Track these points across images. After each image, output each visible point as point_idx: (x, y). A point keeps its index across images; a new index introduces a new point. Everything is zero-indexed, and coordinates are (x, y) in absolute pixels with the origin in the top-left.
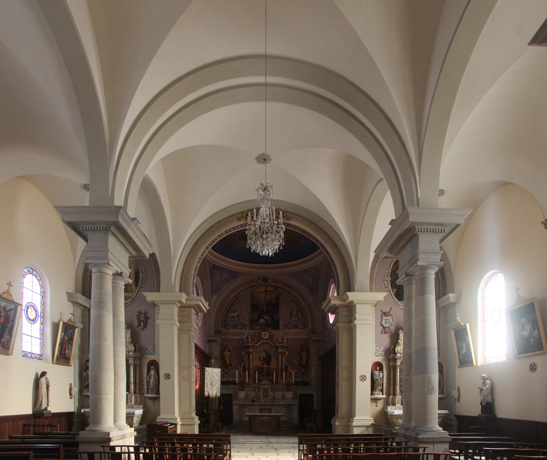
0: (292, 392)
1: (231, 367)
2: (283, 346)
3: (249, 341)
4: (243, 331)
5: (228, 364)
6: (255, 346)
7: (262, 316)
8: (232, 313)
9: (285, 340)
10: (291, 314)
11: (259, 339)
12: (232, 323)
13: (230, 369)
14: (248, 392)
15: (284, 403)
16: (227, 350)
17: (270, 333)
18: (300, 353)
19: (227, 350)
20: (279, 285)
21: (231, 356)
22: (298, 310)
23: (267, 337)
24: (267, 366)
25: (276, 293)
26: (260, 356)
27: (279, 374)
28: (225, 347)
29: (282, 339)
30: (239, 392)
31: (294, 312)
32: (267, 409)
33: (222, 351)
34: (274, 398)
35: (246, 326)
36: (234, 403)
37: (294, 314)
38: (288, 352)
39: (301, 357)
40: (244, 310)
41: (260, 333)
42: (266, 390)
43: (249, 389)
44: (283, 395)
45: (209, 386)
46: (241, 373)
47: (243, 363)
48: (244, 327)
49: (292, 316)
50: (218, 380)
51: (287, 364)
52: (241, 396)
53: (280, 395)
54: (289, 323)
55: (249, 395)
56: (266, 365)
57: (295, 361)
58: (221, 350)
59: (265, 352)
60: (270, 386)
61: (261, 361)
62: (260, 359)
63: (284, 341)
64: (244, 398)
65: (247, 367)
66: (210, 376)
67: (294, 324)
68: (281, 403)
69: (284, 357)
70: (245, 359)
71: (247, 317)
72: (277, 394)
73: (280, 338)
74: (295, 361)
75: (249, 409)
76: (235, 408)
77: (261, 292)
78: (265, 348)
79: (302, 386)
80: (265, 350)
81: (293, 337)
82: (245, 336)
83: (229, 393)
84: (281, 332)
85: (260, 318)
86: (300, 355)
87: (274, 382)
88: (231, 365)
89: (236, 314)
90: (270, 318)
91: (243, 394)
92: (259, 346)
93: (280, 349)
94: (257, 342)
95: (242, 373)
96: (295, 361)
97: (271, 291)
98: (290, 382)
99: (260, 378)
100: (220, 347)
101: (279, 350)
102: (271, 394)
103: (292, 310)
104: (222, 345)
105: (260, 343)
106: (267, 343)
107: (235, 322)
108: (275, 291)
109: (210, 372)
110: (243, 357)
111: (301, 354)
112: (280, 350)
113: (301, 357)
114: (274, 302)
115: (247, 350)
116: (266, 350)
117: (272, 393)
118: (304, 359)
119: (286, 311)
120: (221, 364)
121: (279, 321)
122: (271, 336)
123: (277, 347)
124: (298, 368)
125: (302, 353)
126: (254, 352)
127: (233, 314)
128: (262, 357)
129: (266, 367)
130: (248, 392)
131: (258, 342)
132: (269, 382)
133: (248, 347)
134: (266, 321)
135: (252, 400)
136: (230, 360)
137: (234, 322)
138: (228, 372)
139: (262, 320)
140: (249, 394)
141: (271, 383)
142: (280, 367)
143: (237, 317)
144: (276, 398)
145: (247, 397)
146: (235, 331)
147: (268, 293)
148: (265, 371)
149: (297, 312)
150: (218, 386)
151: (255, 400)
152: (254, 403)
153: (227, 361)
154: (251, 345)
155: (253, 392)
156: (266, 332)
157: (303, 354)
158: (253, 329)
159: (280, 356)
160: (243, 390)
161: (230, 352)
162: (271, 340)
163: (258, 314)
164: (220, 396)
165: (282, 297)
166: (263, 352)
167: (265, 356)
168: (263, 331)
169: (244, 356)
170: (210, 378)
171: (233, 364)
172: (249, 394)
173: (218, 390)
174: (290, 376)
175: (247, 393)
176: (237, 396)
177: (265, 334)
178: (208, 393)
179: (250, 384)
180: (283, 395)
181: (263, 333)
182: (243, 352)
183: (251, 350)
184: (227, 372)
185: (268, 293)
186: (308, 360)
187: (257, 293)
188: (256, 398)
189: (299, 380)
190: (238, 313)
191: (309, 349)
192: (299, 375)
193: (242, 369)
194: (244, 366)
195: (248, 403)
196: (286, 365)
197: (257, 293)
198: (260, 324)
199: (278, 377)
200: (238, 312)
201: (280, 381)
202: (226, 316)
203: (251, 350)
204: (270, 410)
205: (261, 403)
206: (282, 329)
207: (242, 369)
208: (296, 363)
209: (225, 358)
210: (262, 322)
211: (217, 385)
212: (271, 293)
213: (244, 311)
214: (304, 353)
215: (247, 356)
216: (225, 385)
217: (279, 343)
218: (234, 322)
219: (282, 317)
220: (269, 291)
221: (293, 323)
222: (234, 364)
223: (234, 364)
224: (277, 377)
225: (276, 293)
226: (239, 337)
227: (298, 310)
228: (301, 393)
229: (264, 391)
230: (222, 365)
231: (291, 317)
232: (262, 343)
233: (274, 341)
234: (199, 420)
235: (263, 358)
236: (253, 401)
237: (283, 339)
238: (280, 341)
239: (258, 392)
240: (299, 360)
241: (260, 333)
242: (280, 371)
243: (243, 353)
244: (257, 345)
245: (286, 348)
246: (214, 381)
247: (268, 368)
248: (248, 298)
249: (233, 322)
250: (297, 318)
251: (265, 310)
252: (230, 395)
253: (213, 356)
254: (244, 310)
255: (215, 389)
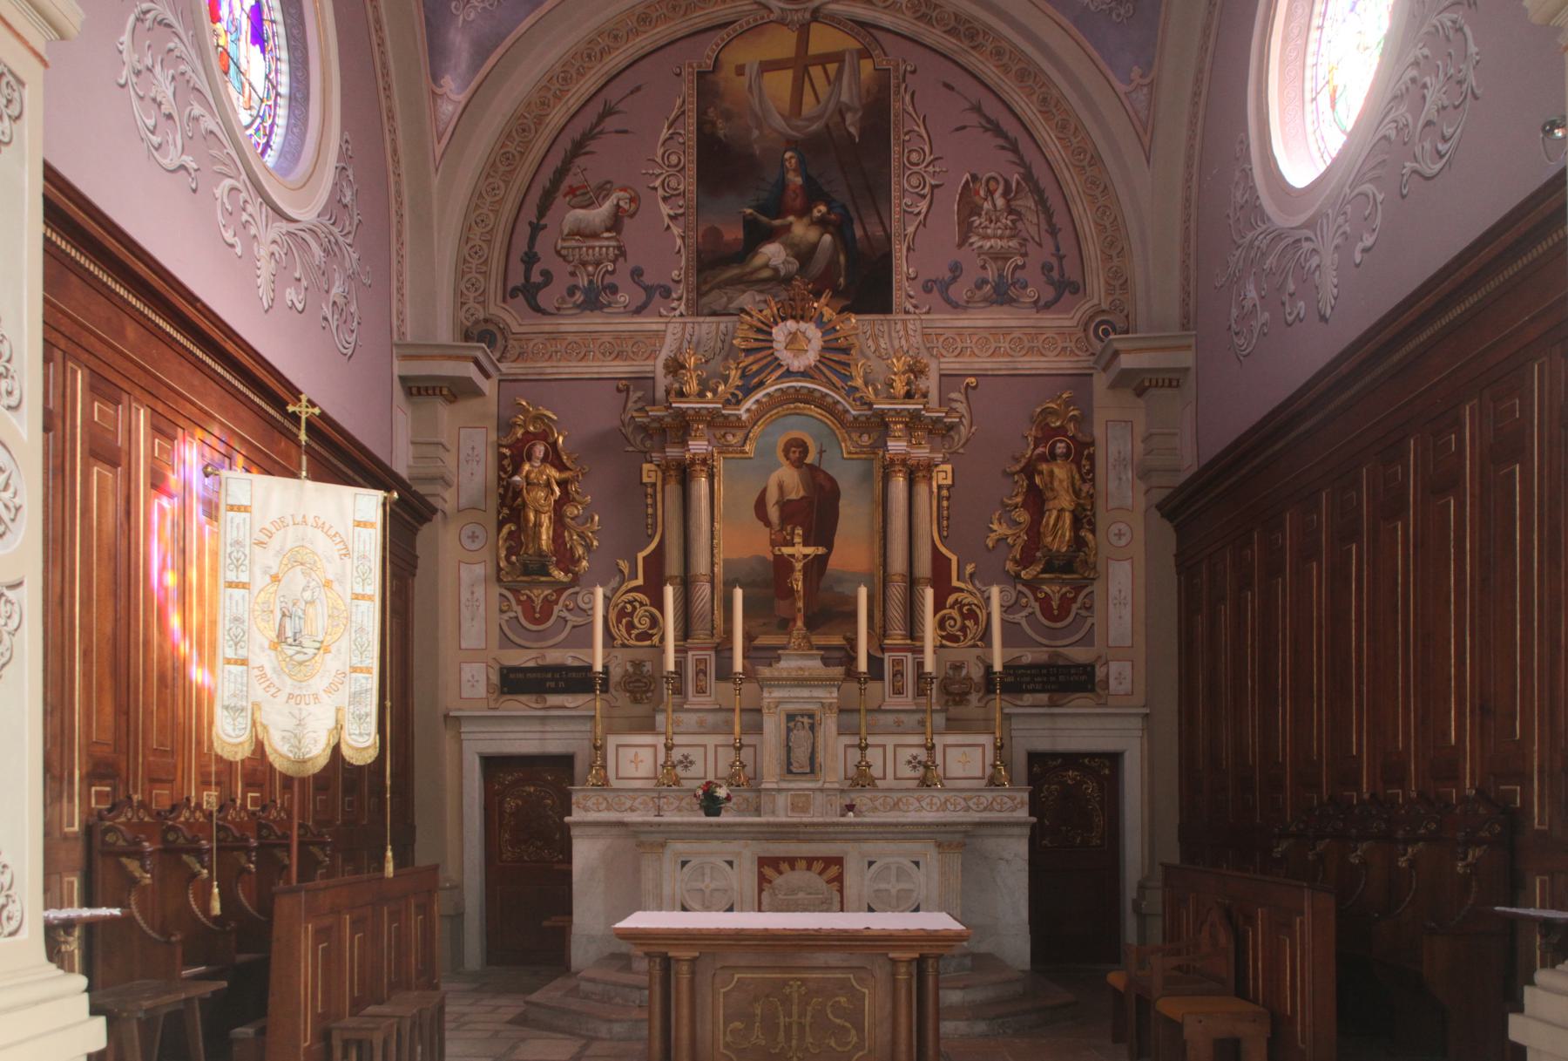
0: (985, 739)
1: (567, 572)
2: (915, 416)
3: (686, 389)
4: (649, 323)
5: (544, 547)
6: (726, 417)
7: (777, 222)
8: (574, 207)
9: (930, 383)
10: (968, 207)
11: (755, 368)
12: (573, 274)
13: (560, 588)
14: (678, 740)
15: (929, 816)
16: (540, 450)
17: (827, 329)
18: (1029, 470)
19: (540, 450)
20: (886, 20)
21: (566, 498)
22: (1015, 178)
23: (811, 358)
24: (810, 550)
25: (867, 67)
26: (764, 491)
27: (896, 613)
28: (527, 433)
29: (911, 371)
30: (612, 740)
31: (991, 193)
32: (810, 861)
33: (506, 462)
34: (862, 779)
35: (666, 293)
36: (576, 816)
37: (987, 206)
38: (948, 467)
39: (1036, 500)
40: (657, 183)
41: (759, 330)
42: (806, 720)
43: (689, 719)
44: (922, 755)
45: (263, 658)
46: (631, 615)
47: (651, 537)
48: (653, 295)
49: (976, 220)
50: (356, 597)
51: (943, 550)
52: (628, 769)
53: (906, 754)
54: (956, 269)
55: (687, 762)
56: (806, 544)
57: (1000, 529)
58: (502, 457)
59: (799, 464)
60: (830, 695)
61: (768, 523)
62: (760, 507)
63: (922, 384)
64: (650, 784)
65: (673, 566)
66: (268, 559)
67: (991, 274)
68: (912, 817)
69: (922, 490)
70: (660, 512)
71: (676, 230)
72: (880, 750)
73: (898, 366)
74: (1000, 529)
75: (684, 864)
76: (585, 853)
77: (768, 66)
78: (796, 434)
79: (1044, 697)
80: (796, 451)
81: (984, 363)
82: (660, 362)
83: (554, 746)
84: (899, 326)
85: (757, 235)
86: (1032, 486)
87: (863, 666)
88: (567, 560)
89: (599, 214)
90: (827, 238)
91: (646, 754)
92: (756, 417)
93: (898, 438)
94: (740, 395)
95: (640, 611)
96: (995, 527)
97: (838, 57)
98: (964, 672)
99: (763, 641)
100: (493, 436)
101: (891, 444)
102: (836, 751)
103: (974, 178)
104: (505, 426)
105: (759, 395)
106: (809, 398)
107: (597, 264)
108: (865, 54)
109: (274, 515)
110: (649, 501)
111: (1037, 480)
112: (896, 446)
113: (1036, 500)
114: (852, 130)
115: (673, 452)
116: (803, 448)
117: (847, 746)
118: (1061, 510)
119: (933, 187)
120: (503, 554)
121: (887, 257)
122: (837, 354)
123: (879, 425)
124: (1018, 576)
125: (1044, 467)
126: (720, 464)
127: (580, 213)
128: (772, 496)
129: (806, 556)
130: (678, 740)
131: (748, 391)
132: (826, 662)
133: (683, 427)
134: (804, 255)
135: (700, 792)
136: (559, 522)
137: (590, 269)
138: (548, 604)
139: (773, 253)
140: (685, 751)
141: (838, 671)
142: (898, 563)
143: (608, 230)
144: (872, 781)
145: (668, 777)
146: (593, 322)
147: (816, 72)
148: (799, 586)
149: (1005, 194)
150: (356, 661)
151: (722, 792)
152: (717, 814)
153: (538, 525)
154: (697, 412)
155: (711, 740)
156: (803, 325)
157: (1051, 473)
158: (714, 314)
159: (899, 483)
160: (648, 727)
161: (561, 467)
162: (834, 379)
163: (749, 211)
164: (381, 758)
165: (908, 98)
166: (782, 459)
167: (796, 492)
168: (784, 319)
169: (654, 496)
170: (276, 579)
171: (580, 551)
172: (685, 751)
173: (355, 698)
174: (964, 629)
175: (669, 748)
176: (604, 767)
177: (793, 338)
178: (244, 721)
179: (691, 688)
180: (922, 755)
181: (780, 333)
182: (646, 466)
183: (698, 446)
184: (538, 603)
185: (816, 72)
186: (1083, 518)
187: (740, 70)
188: (731, 781)
189: (1028, 656)
190: (618, 206)
191: (1092, 444)
192: (1024, 623)
193: (640, 581)
194: (656, 563)
195: (677, 819)
196: (936, 553)
197: (740, 70)
198: (766, 274)
199: (885, 635)
200: (612, 200)
201: (897, 662)
202: (536, 229)
203: (698, 446)
204: (834, 870)
205: (771, 819)
206: (907, 312)
207: (640, 581)
208: (1002, 539)
209: (524, 505)
210: (775, 262)
211: (344, 644)
212: (832, 68)
213: (655, 189)
214: (1056, 471)
215: (673, 489)
216: (523, 698)
217: (892, 398)
218: (590, 269)
219: (910, 230)
220: (824, 60)
221: (984, 268)
222: (588, 547)
223: (588, 547)
224: (879, 632)
225: (867, 67)
226: (620, 368)
227: (1015, 178)
228: (1043, 745)
229: (789, 730)
230: (507, 559)
231: (966, 230)
232: (775, 402)
233: (859, 382)
234: (95, 1011)
235: (785, 505)
236: (711, 804)
237: (917, 370)
238: (900, 387)
239: (746, 740)
240: (1023, 517)
241: (759, 330)
242: (897, 591)
243: (649, 473)
244: (742, 412)
245: (939, 431)
246: (311, 602)
247: (816, 567)
248: (679, 102)
249: (584, 264)
250: (1008, 232)
251: (796, 180)
252: (564, 762)
253: (449, 494)
254: (657, 183)
255: (319, 684)
